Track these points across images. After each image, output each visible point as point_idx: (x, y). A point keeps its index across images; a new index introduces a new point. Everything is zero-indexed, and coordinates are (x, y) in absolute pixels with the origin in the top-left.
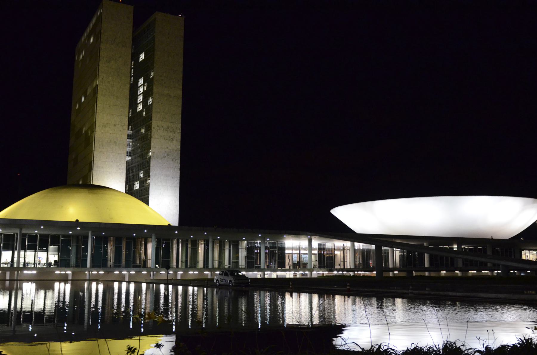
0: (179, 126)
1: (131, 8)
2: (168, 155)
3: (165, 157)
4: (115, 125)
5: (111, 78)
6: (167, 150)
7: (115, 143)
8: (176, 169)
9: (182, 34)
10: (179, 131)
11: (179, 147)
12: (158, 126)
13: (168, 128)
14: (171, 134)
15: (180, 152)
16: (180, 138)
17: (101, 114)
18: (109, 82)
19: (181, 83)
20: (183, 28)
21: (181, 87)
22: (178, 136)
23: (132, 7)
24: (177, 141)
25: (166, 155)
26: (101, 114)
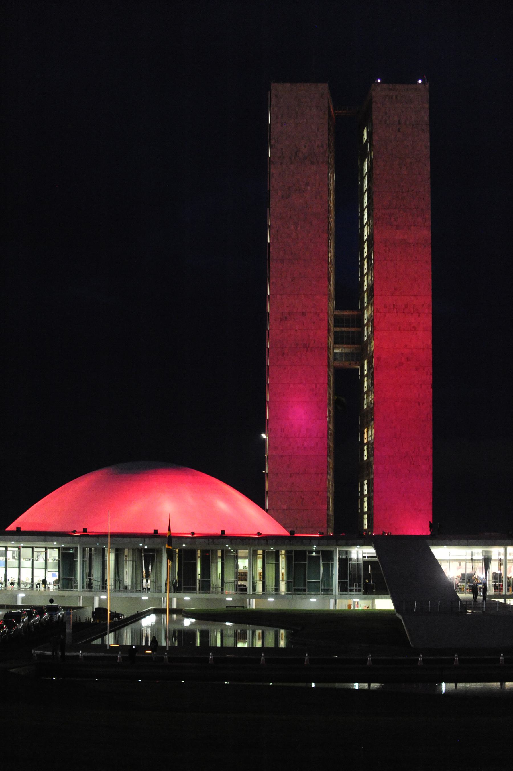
1: (323, 88)
2: (408, 359)
4: (303, 314)
9: (426, 118)
10: (428, 310)
11: (430, 342)
12: (385, 307)
13: (406, 307)
15: (430, 351)
16: (430, 323)
17: (278, 297)
19: (428, 215)
20: (427, 106)
21: (429, 223)
23: (326, 85)
26: (278, 297)
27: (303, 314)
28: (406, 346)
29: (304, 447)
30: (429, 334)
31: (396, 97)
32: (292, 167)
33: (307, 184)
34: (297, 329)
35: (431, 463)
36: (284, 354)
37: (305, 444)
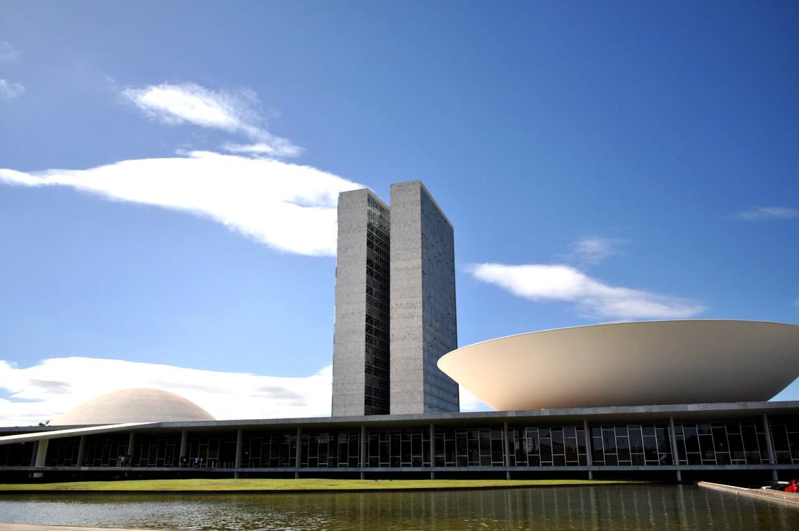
0: (420, 299)
2: (409, 334)
3: (405, 337)
5: (348, 267)
6: (408, 330)
7: (354, 332)
8: (418, 349)
11: (421, 323)
13: (408, 304)
14: (411, 311)
15: (422, 328)
18: (346, 272)
20: (419, 191)
21: (421, 256)
22: (420, 311)
24: (418, 317)
25: (406, 335)
27: (353, 314)
28: (407, 327)
29: (352, 390)
30: (421, 319)
31: (403, 189)
32: (349, 235)
33: (356, 243)
34: (349, 322)
35: (423, 395)
36: (342, 337)
37: (353, 387)
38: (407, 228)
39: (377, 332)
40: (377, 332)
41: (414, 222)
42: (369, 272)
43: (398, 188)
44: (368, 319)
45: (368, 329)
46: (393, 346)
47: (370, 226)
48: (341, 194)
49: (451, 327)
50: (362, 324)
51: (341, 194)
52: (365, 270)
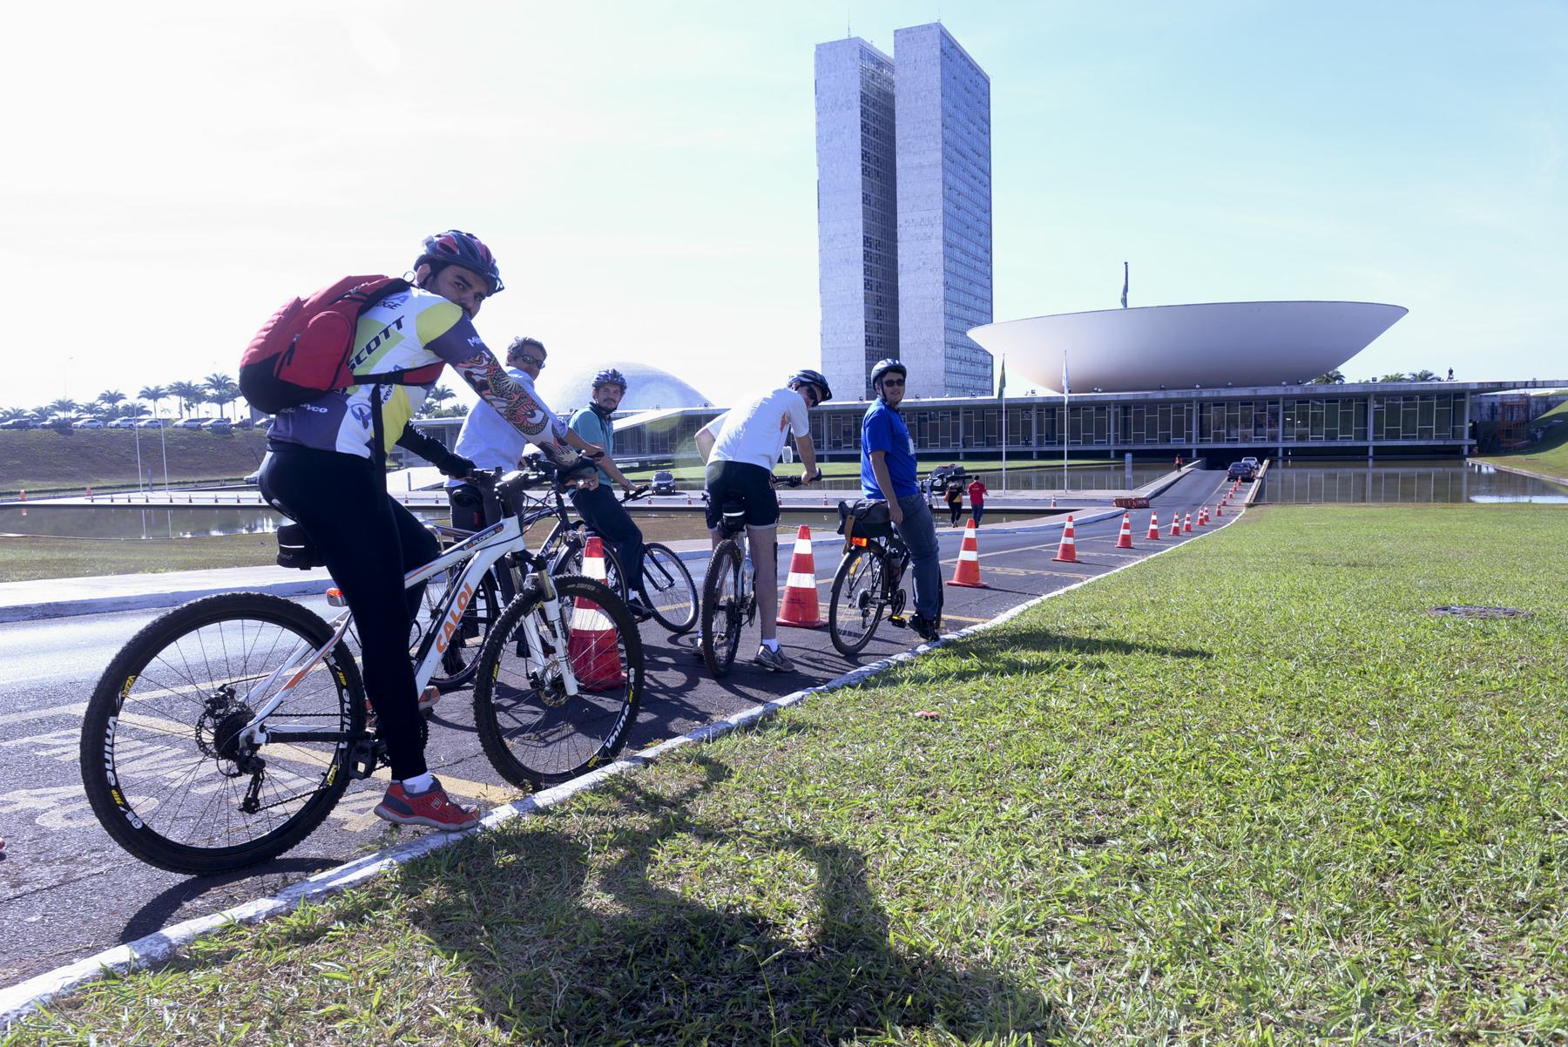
14: (927, 230)
19: (939, 140)
22: (939, 230)
38: (920, 103)
39: (879, 259)
40: (879, 259)
41: (931, 92)
42: (865, 170)
43: (904, 37)
44: (867, 241)
45: (867, 256)
46: (903, 281)
47: (864, 97)
48: (819, 47)
49: (982, 201)
50: (859, 250)
51: (819, 47)
52: (860, 169)
